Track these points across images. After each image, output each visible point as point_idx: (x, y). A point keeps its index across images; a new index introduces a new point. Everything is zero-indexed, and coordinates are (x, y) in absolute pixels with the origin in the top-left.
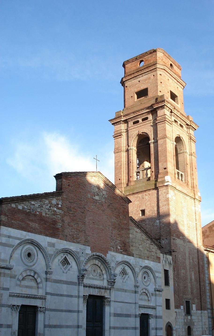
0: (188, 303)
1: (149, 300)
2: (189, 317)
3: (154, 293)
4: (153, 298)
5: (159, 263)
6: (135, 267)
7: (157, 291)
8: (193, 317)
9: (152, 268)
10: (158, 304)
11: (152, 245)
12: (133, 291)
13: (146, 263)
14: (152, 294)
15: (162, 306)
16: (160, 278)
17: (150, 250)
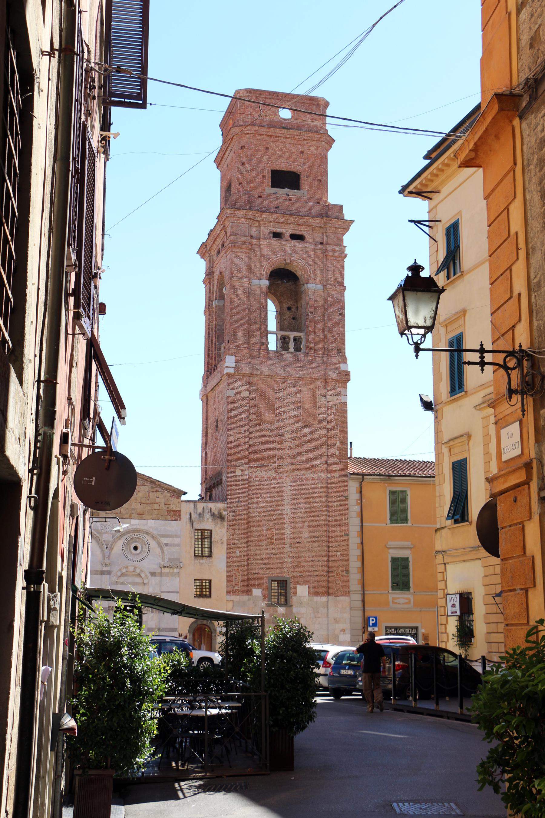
0: (283, 584)
1: (144, 584)
2: (281, 610)
3: (159, 570)
4: (154, 581)
5: (176, 520)
6: (101, 534)
7: (164, 567)
8: (295, 610)
9: (151, 530)
10: (163, 590)
11: (157, 491)
12: (97, 571)
13: (133, 525)
14: (153, 574)
15: (177, 592)
16: (178, 545)
17: (148, 502)
